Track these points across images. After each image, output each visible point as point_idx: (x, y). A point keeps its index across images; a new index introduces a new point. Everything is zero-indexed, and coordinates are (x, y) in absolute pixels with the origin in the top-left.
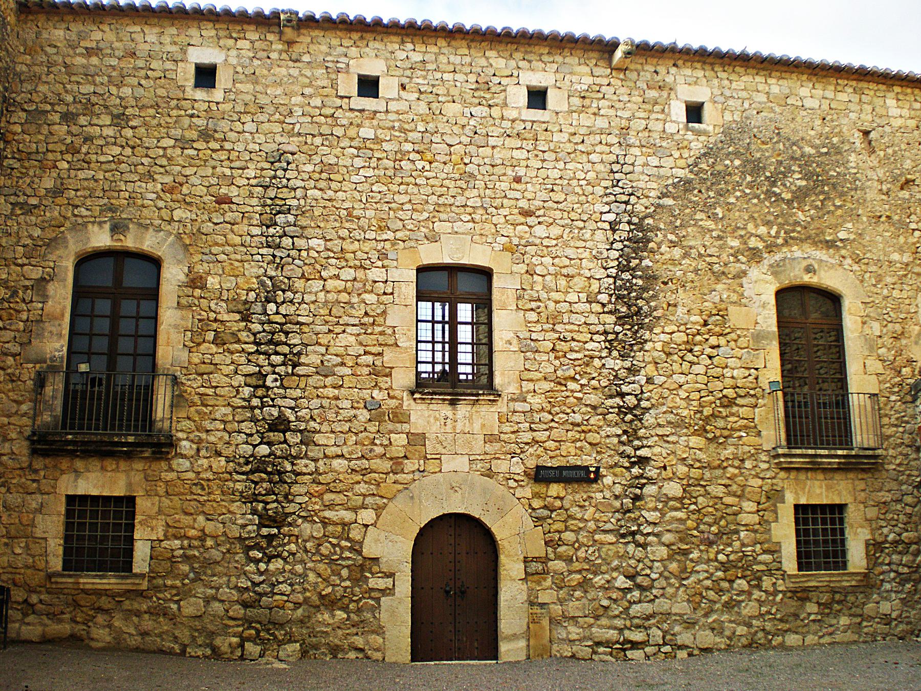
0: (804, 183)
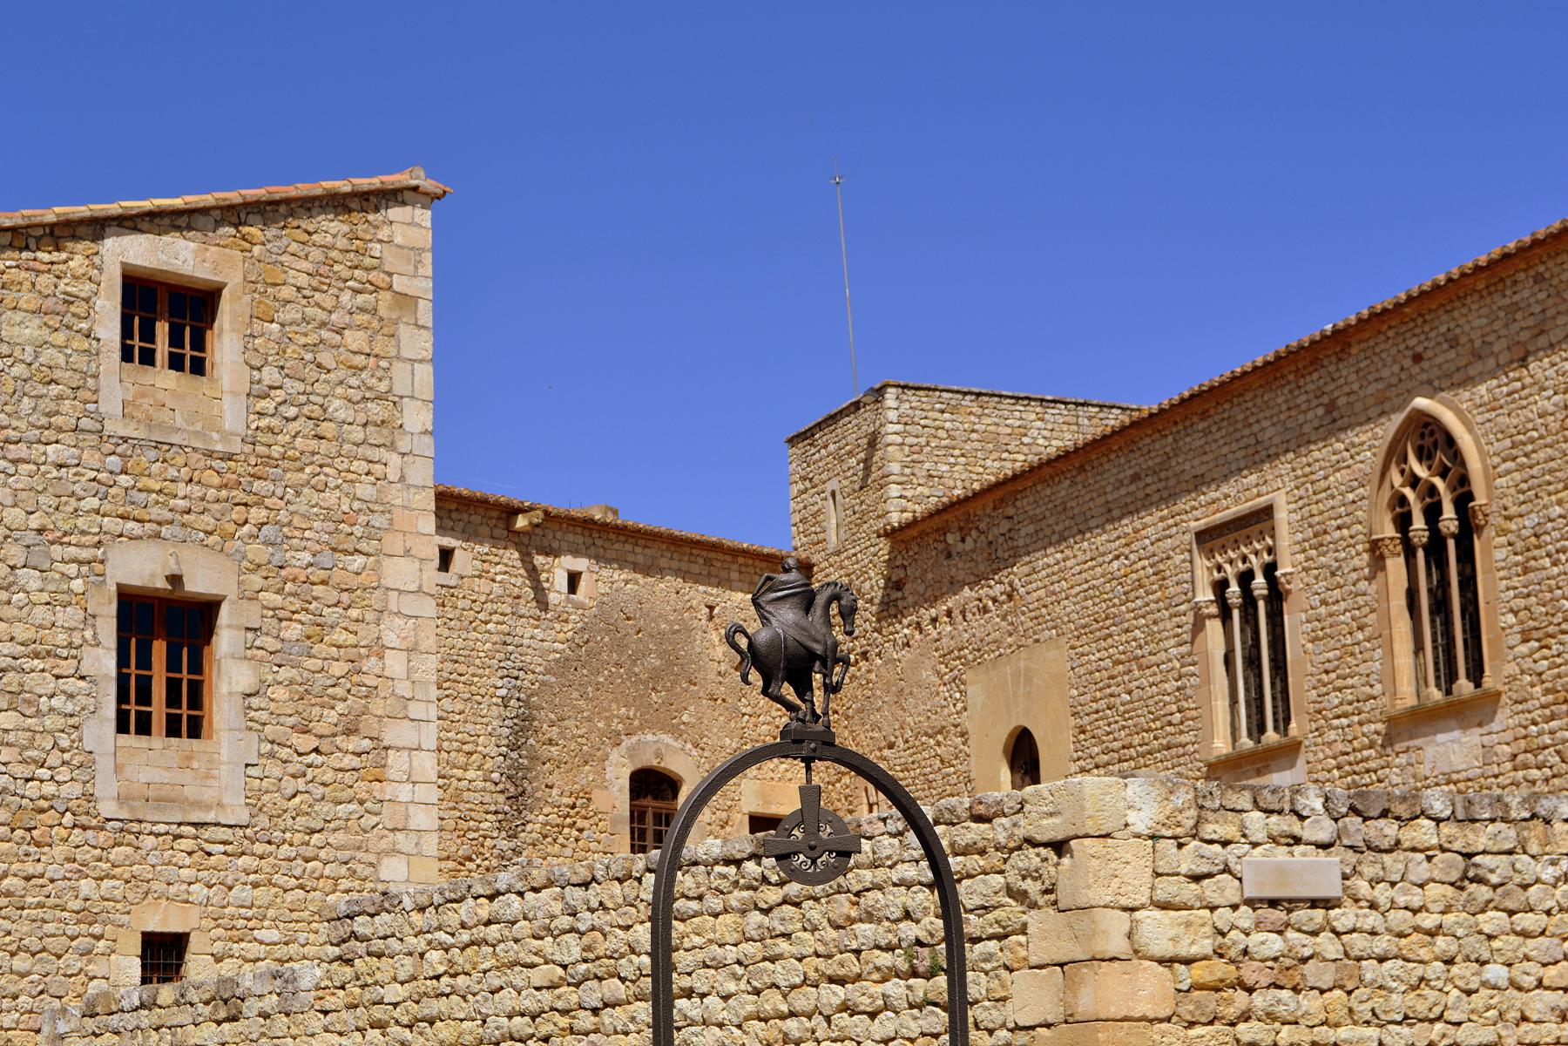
0: (658, 663)
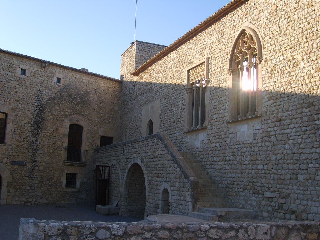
0: (80, 100)
